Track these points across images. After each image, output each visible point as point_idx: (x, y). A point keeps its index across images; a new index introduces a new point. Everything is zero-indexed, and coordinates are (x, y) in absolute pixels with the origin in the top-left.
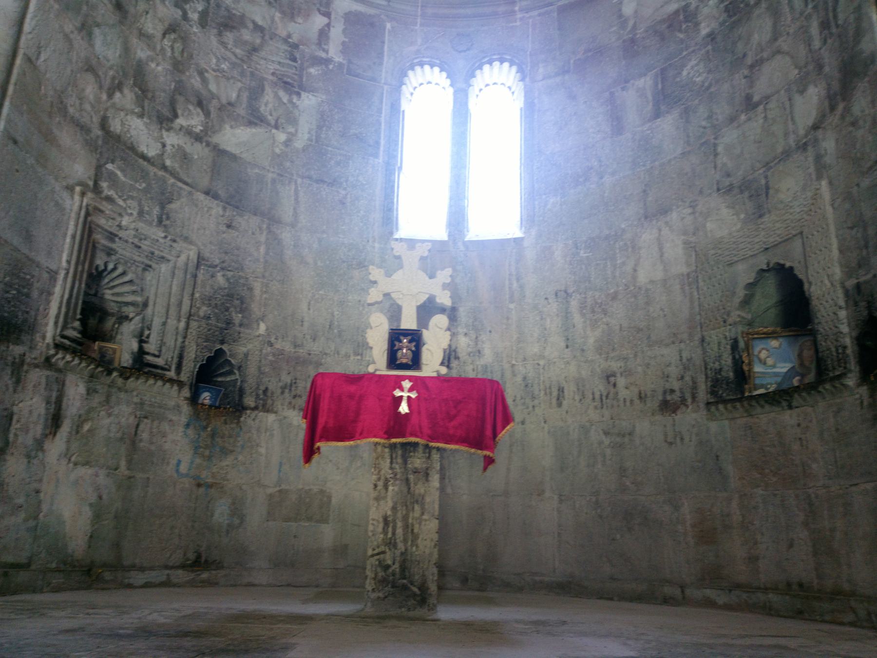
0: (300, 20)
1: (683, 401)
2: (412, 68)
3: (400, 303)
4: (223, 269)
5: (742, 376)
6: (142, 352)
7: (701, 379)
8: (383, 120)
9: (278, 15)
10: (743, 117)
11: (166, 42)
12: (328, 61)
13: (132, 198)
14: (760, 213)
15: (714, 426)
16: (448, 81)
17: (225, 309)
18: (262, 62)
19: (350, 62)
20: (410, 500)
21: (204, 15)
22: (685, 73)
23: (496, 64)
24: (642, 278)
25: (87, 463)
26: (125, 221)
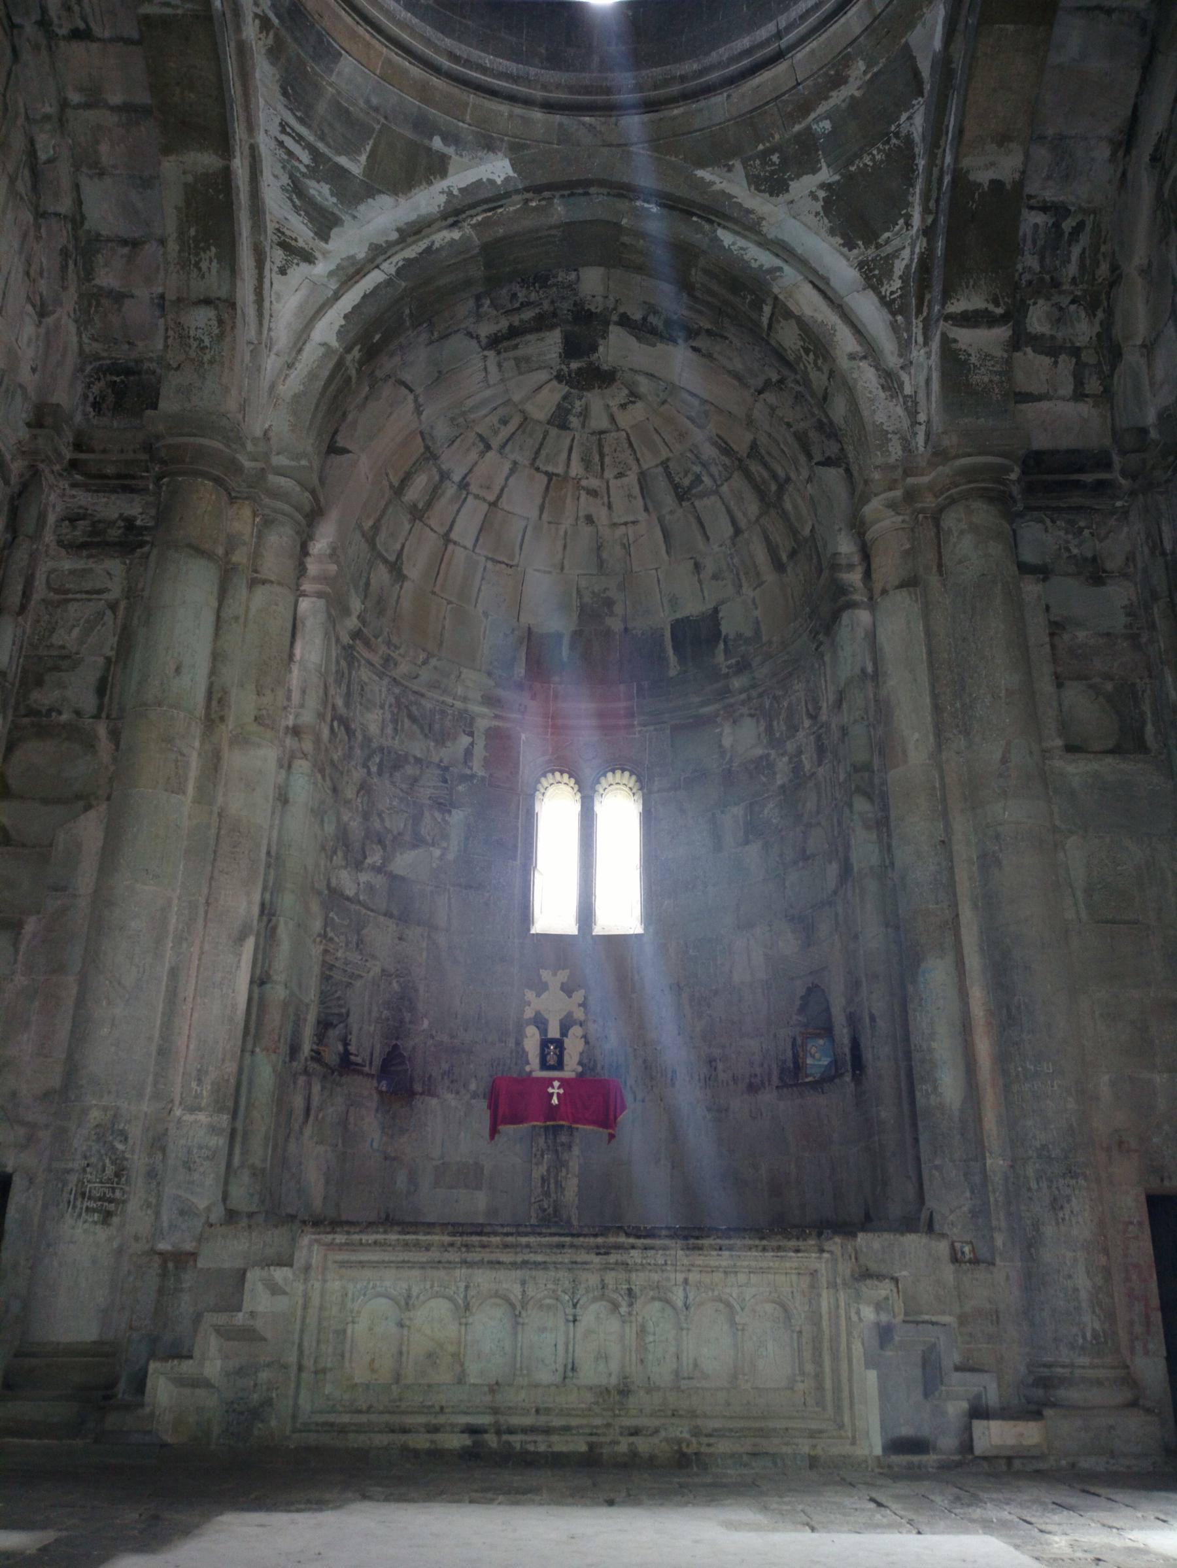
0: (449, 744)
1: (763, 1083)
2: (544, 775)
3: (546, 1016)
4: (397, 976)
5: (798, 1067)
6: (347, 1053)
7: (774, 1066)
8: (520, 825)
9: (432, 744)
10: (801, 864)
11: (359, 800)
12: (473, 776)
13: (342, 934)
16: (576, 787)
18: (422, 790)
19: (491, 775)
20: (559, 1164)
21: (380, 765)
22: (766, 812)
23: (618, 773)
25: (321, 1143)
26: (339, 954)
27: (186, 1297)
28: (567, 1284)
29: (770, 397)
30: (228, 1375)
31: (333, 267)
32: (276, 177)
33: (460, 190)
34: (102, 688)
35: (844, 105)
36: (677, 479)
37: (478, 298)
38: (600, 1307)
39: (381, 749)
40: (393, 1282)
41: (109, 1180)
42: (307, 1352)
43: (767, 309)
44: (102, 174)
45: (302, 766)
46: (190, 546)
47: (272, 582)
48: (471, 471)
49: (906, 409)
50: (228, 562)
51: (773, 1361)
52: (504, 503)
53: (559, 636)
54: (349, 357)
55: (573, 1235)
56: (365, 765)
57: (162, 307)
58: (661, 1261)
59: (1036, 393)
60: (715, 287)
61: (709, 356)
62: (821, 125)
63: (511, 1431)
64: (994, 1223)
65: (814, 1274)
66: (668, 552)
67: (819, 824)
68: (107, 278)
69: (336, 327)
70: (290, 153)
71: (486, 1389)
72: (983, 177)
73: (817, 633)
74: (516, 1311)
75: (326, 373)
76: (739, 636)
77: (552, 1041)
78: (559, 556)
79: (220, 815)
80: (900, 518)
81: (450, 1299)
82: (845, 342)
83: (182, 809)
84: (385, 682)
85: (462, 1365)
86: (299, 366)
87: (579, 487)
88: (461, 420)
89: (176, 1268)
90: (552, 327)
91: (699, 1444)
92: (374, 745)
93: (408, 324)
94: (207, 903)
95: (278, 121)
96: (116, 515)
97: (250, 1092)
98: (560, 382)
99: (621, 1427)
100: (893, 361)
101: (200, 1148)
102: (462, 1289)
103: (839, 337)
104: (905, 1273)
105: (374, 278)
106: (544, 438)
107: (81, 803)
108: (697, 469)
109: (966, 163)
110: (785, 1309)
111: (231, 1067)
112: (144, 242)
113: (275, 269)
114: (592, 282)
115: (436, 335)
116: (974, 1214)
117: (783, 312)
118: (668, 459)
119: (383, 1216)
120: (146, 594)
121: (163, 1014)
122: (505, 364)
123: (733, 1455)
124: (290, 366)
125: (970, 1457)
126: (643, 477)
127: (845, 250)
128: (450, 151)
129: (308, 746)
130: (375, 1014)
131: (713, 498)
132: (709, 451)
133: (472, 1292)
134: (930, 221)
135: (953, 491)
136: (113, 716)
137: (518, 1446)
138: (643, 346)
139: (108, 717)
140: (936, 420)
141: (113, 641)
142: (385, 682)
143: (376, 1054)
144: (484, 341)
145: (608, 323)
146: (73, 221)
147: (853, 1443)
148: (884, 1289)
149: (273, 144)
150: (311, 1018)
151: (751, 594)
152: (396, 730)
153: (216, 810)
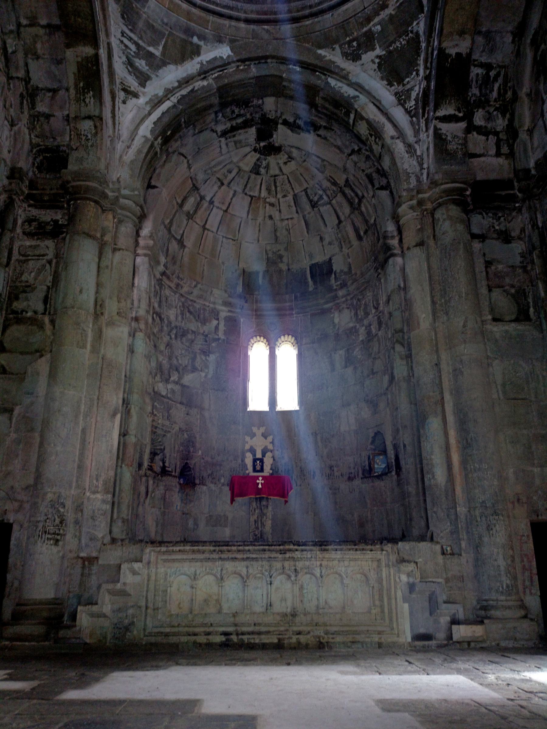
0: (207, 324)
1: (355, 477)
2: (252, 338)
5: (371, 469)
9: (200, 324)
12: (219, 339)
14: (375, 412)
15: (364, 486)
17: (188, 447)
23: (286, 336)
24: (342, 429)
25: (154, 507)
26: (160, 422)
27: (94, 578)
28: (267, 567)
29: (354, 157)
30: (114, 612)
31: (148, 99)
32: (120, 57)
33: (207, 62)
34: (46, 300)
35: (387, 18)
36: (311, 198)
37: (216, 113)
38: (283, 577)
39: (176, 327)
40: (188, 568)
41: (57, 525)
42: (149, 600)
43: (352, 116)
44: (38, 58)
45: (140, 335)
46: (84, 233)
47: (123, 250)
48: (214, 195)
49: (418, 162)
50: (102, 241)
51: (361, 601)
52: (230, 210)
53: (258, 273)
54: (156, 143)
55: (269, 545)
56: (169, 335)
57: (68, 120)
58: (309, 556)
59: (478, 153)
60: (327, 105)
61: (325, 138)
62: (376, 28)
63: (243, 634)
64: (461, 537)
65: (379, 561)
66: (308, 232)
67: (379, 358)
68: (42, 108)
69: (150, 128)
70: (126, 46)
71: (231, 615)
72: (453, 52)
73: (378, 269)
74: (244, 580)
75: (145, 150)
76: (342, 271)
77: (258, 459)
78: (257, 235)
79: (103, 358)
80: (416, 214)
81: (215, 576)
82: (389, 131)
83: (85, 355)
84: (177, 295)
85: (220, 605)
86: (133, 147)
87: (265, 202)
88: (209, 171)
89: (89, 564)
90: (251, 126)
91: (328, 638)
92: (173, 325)
93: (183, 126)
94: (98, 399)
95: (120, 31)
96: (50, 220)
97: (120, 485)
98: (256, 152)
99: (293, 631)
100: (411, 139)
101: (99, 510)
102: (219, 571)
103: (386, 129)
104: (420, 560)
105: (167, 105)
106: (249, 179)
107: (38, 354)
108: (321, 192)
109: (444, 45)
110: (365, 576)
111: (112, 473)
112: (59, 90)
113: (120, 101)
114: (270, 104)
115: (197, 131)
116: (452, 533)
117: (359, 117)
118: (307, 188)
119: (183, 539)
120: (65, 256)
121: (80, 450)
122: (229, 144)
123: (343, 643)
124: (129, 147)
125: (451, 642)
126: (295, 197)
127: (388, 87)
128: (202, 43)
129: (142, 326)
130: (176, 449)
131: (328, 206)
132: (326, 184)
133: (224, 572)
134: (428, 72)
135: (440, 200)
136: (52, 313)
137: (246, 641)
138: (294, 135)
139: (49, 313)
140: (432, 167)
141: (50, 278)
142: (177, 295)
143: (178, 466)
144: (219, 134)
145: (277, 124)
146: (25, 80)
147: (398, 636)
148: (411, 567)
149: (118, 42)
150: (148, 451)
151: (347, 251)
152: (183, 318)
153: (101, 356)
